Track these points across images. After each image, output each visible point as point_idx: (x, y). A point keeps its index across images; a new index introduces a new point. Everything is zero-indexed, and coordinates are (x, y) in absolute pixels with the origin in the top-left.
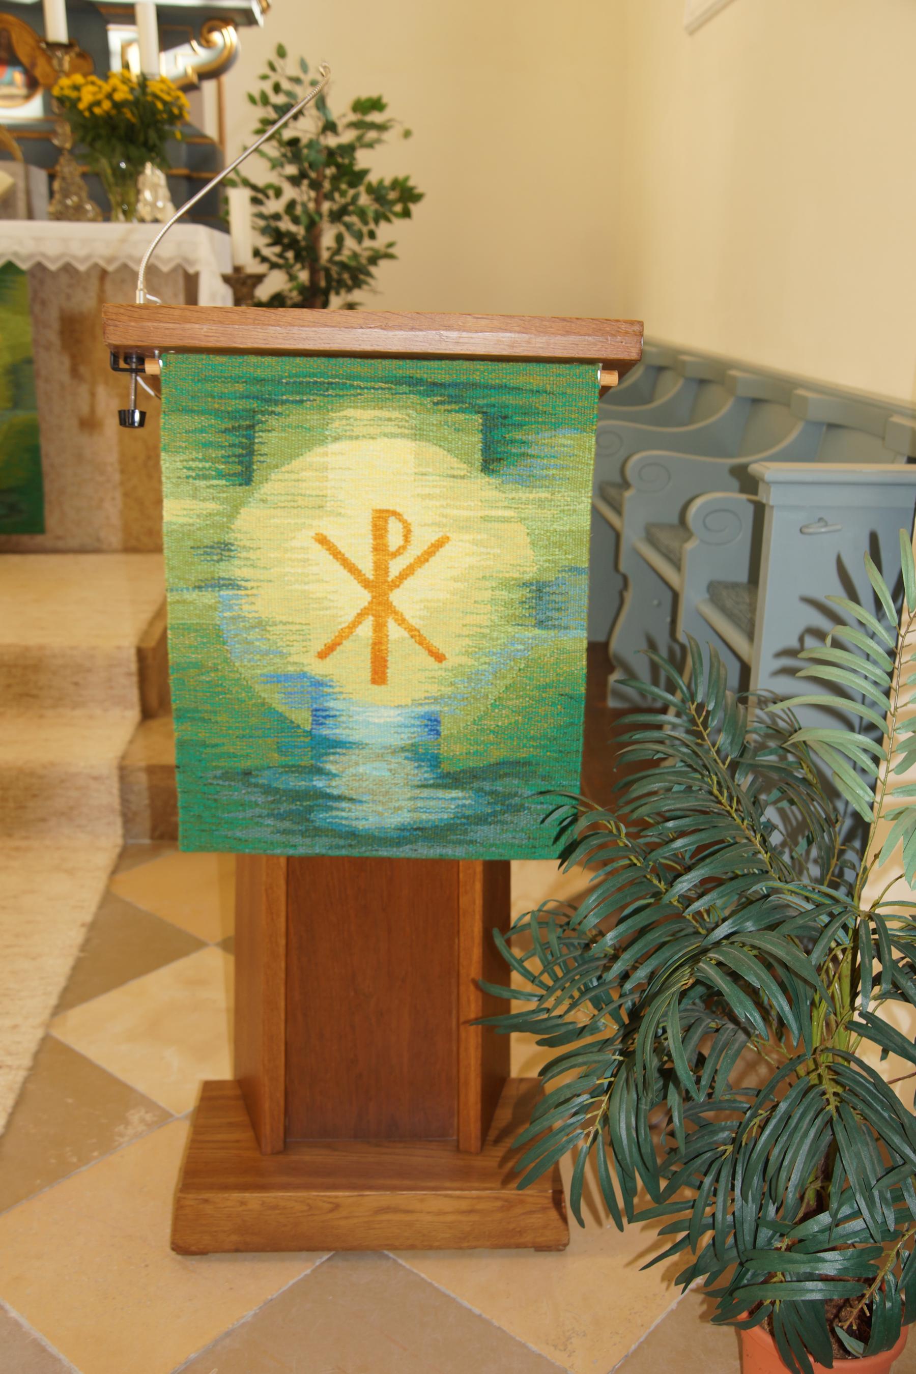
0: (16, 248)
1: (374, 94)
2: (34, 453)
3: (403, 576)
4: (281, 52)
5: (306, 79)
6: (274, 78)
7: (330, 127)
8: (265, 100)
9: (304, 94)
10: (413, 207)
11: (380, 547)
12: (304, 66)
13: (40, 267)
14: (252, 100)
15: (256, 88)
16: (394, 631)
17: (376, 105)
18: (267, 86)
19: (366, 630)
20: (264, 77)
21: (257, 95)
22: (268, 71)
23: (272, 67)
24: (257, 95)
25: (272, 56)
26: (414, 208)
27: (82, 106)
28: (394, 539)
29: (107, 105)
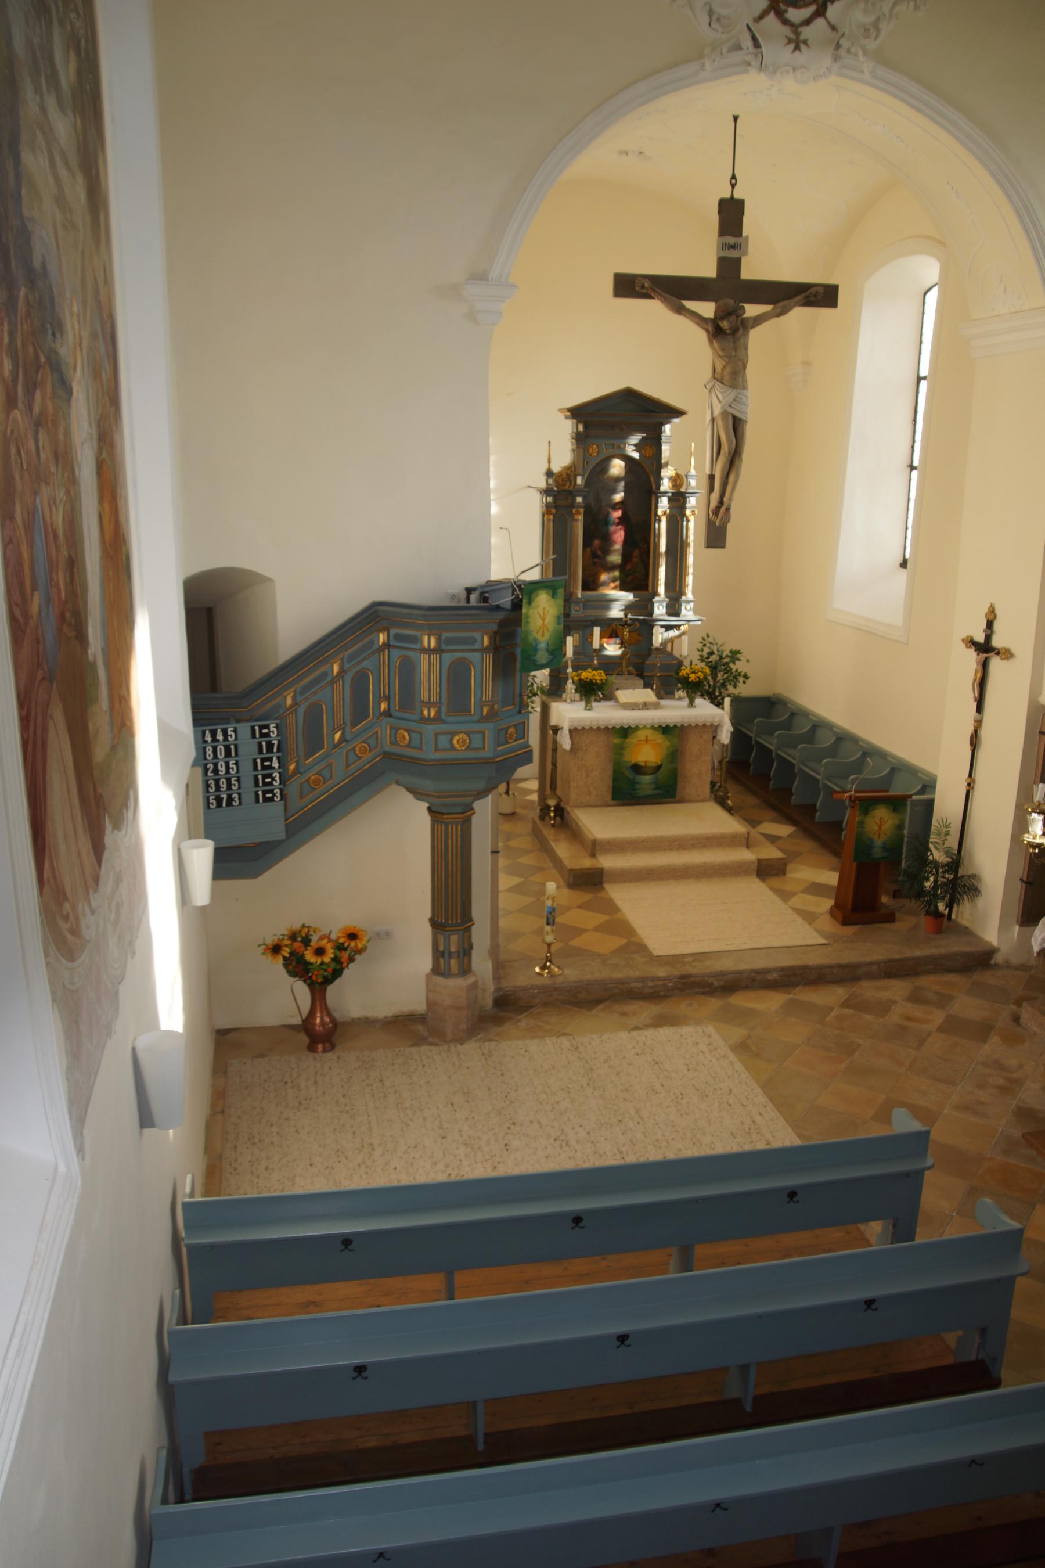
1: (738, 650)
2: (676, 775)
3: (884, 824)
4: (708, 636)
6: (704, 642)
7: (721, 658)
9: (715, 651)
10: (747, 681)
11: (881, 822)
12: (714, 640)
13: (682, 726)
14: (698, 650)
15: (700, 646)
16: (881, 832)
17: (739, 652)
18: (701, 645)
19: (878, 832)
20: (701, 643)
21: (700, 648)
22: (701, 640)
23: (704, 639)
24: (700, 648)
25: (705, 636)
26: (747, 681)
27: (690, 680)
28: (882, 820)
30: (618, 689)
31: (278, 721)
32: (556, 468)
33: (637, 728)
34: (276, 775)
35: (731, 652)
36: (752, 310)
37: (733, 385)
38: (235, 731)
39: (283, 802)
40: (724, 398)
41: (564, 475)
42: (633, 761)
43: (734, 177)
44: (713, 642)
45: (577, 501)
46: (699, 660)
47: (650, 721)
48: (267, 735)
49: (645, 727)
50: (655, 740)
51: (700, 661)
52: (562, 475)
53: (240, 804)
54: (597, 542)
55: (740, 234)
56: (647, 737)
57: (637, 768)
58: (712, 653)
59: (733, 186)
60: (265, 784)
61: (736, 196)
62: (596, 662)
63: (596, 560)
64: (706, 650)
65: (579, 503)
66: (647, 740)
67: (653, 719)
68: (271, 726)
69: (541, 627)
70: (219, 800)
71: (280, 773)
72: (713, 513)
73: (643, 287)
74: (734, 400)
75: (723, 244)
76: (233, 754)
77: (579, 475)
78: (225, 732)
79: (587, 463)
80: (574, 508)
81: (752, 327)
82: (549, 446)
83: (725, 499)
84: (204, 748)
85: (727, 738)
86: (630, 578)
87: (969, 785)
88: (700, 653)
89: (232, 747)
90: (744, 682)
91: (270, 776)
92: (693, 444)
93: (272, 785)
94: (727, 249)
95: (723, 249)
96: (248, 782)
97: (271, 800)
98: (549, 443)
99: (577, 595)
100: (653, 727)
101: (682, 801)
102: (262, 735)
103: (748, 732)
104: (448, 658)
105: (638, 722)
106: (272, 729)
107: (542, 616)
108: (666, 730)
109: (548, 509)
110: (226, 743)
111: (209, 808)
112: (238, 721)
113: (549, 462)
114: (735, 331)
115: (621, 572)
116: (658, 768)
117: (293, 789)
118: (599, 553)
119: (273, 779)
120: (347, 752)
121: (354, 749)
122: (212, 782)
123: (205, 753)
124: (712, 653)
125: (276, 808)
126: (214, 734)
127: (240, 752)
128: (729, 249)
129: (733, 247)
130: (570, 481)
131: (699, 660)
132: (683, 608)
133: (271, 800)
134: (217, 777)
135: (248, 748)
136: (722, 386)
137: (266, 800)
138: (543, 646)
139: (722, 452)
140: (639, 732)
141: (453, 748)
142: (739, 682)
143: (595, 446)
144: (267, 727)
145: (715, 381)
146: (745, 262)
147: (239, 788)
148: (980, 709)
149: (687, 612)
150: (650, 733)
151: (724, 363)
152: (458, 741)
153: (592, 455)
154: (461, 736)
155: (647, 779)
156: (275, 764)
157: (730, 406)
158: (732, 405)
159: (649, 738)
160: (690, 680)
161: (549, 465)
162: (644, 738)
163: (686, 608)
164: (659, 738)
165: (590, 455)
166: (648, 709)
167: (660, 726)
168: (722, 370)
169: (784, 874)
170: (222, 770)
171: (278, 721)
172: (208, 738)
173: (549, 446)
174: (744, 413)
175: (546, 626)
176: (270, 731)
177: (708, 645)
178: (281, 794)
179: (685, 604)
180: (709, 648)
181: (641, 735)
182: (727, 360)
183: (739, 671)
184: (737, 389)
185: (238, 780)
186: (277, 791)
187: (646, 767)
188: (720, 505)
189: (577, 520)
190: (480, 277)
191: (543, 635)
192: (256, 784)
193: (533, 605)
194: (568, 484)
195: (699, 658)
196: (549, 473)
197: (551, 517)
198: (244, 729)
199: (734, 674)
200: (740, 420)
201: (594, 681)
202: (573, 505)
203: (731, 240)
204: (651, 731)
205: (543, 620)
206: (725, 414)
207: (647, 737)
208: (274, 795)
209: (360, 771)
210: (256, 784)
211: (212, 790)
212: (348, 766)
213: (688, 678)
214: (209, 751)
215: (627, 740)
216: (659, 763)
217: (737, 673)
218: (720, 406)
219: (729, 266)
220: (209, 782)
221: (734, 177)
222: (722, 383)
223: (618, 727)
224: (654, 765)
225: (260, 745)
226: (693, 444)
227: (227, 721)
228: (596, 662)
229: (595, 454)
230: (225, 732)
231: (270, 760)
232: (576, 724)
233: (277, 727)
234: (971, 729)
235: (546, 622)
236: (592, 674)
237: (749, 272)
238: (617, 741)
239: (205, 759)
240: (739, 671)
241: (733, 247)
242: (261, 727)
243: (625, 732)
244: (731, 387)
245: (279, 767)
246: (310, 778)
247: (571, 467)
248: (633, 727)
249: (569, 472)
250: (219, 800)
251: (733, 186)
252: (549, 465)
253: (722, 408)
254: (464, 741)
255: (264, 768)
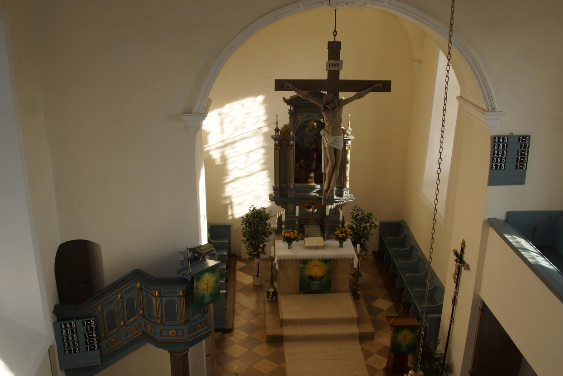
0: (331, 257)
4: (356, 207)
5: (360, 210)
6: (355, 209)
8: (353, 213)
9: (360, 212)
12: (360, 208)
14: (351, 213)
15: (352, 211)
20: (353, 209)
23: (354, 208)
25: (355, 207)
27: (339, 237)
29: (343, 237)
30: (307, 237)
31: (94, 318)
32: (280, 127)
33: (311, 260)
34: (95, 340)
35: (368, 214)
36: (343, 96)
37: (333, 134)
38: (75, 323)
39: (99, 350)
40: (329, 140)
41: (285, 130)
42: (309, 275)
43: (335, 31)
44: (359, 209)
45: (291, 143)
46: (352, 218)
47: (317, 257)
48: (90, 324)
49: (315, 260)
50: (320, 265)
51: (352, 218)
52: (284, 130)
53: (79, 352)
54: (302, 161)
55: (339, 59)
56: (316, 264)
57: (311, 278)
58: (358, 215)
59: (335, 35)
60: (90, 343)
61: (336, 41)
62: (297, 223)
63: (301, 169)
64: (355, 214)
65: (292, 144)
66: (316, 265)
67: (319, 256)
68: (92, 320)
69: (206, 288)
70: (70, 351)
71: (97, 339)
72: (325, 192)
73: (288, 87)
74: (334, 141)
75: (330, 64)
76: (75, 332)
77: (291, 131)
78: (71, 324)
79: (296, 124)
80: (289, 146)
81: (344, 105)
82: (277, 117)
83: (331, 186)
84: (62, 331)
85: (356, 265)
86: (319, 177)
87: (451, 321)
88: (352, 215)
89: (74, 329)
90: (375, 228)
91: (93, 340)
92: (350, 115)
93: (94, 343)
94: (332, 66)
95: (330, 67)
96: (82, 342)
97: (94, 349)
98: (277, 115)
99: (291, 187)
100: (319, 260)
101: (335, 292)
102: (87, 324)
103: (384, 240)
104: (164, 300)
105: (311, 257)
106: (92, 322)
107: (206, 283)
108: (325, 261)
109: (276, 146)
110: (71, 328)
111: (65, 354)
112: (78, 318)
113: (277, 125)
114: (334, 108)
115: (315, 175)
116: (322, 278)
117: (103, 344)
118: (303, 166)
119: (94, 341)
120: (126, 331)
121: (129, 329)
122: (66, 344)
123: (62, 333)
124: (358, 215)
125: (97, 352)
126: (66, 325)
127: (78, 330)
128: (333, 67)
129: (335, 65)
130: (288, 133)
131: (352, 218)
132: (344, 192)
133: (94, 349)
134: (68, 342)
135: (82, 330)
136: (328, 134)
137: (91, 349)
138: (208, 295)
139: (329, 165)
140: (312, 262)
141: (169, 336)
142: (372, 228)
143: (300, 116)
144: (90, 321)
145: (325, 131)
146: (341, 72)
147: (79, 345)
148: (457, 288)
149: (346, 194)
150: (318, 262)
151: (328, 124)
152: (171, 333)
153: (299, 120)
154: (172, 331)
155: (316, 282)
156: (95, 335)
157: (332, 143)
158: (333, 143)
159: (317, 265)
160: (339, 237)
161: (277, 126)
162: (315, 265)
163: (346, 193)
164: (322, 265)
165: (298, 121)
166: (319, 249)
167: (323, 259)
168: (328, 127)
169: (373, 339)
170: (71, 339)
171: (94, 318)
172: (64, 327)
173: (277, 117)
174: (339, 146)
175: (209, 287)
176: (91, 323)
177: (356, 211)
178: (98, 347)
179: (345, 191)
180: (357, 212)
181: (313, 263)
182: (329, 123)
183: (373, 222)
184: (336, 136)
185: (78, 342)
186: (96, 346)
187: (316, 277)
188: (328, 189)
189: (290, 152)
190: (188, 112)
191: (208, 291)
192: (86, 343)
193: (200, 281)
194: (287, 134)
195: (352, 217)
196: (277, 130)
197: (278, 151)
198: (79, 322)
199: (371, 223)
200: (338, 149)
201: (291, 237)
202: (288, 144)
203: (334, 62)
204: (318, 262)
205: (207, 285)
206: (329, 147)
207: (316, 264)
208: (95, 347)
209: (132, 339)
210: (86, 343)
211: (67, 346)
212: (127, 336)
213: (338, 235)
214: (64, 332)
215: (307, 265)
216: (322, 275)
217: (372, 223)
218: (327, 144)
219: (333, 74)
220: (65, 344)
221: (335, 31)
222: (328, 133)
223: (302, 259)
224: (320, 276)
225: (87, 328)
226: (350, 115)
227: (72, 319)
228: (297, 223)
229: (300, 120)
230: (71, 324)
231: (92, 334)
232: (281, 258)
233: (94, 320)
234: (453, 296)
235: (209, 285)
236: (290, 234)
237: (344, 75)
238: (301, 265)
239: (62, 335)
240: (373, 222)
241: (335, 65)
242: (87, 321)
243: (305, 261)
244: (332, 135)
245: (96, 337)
246: (111, 340)
247: (288, 126)
248: (309, 259)
249: (288, 129)
250: (70, 351)
251: (335, 35)
252: (277, 126)
253: (328, 145)
254: (174, 333)
255: (89, 337)
